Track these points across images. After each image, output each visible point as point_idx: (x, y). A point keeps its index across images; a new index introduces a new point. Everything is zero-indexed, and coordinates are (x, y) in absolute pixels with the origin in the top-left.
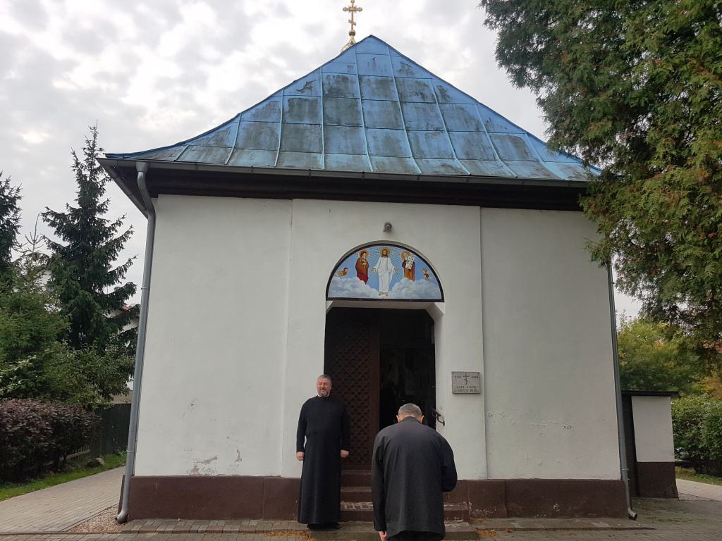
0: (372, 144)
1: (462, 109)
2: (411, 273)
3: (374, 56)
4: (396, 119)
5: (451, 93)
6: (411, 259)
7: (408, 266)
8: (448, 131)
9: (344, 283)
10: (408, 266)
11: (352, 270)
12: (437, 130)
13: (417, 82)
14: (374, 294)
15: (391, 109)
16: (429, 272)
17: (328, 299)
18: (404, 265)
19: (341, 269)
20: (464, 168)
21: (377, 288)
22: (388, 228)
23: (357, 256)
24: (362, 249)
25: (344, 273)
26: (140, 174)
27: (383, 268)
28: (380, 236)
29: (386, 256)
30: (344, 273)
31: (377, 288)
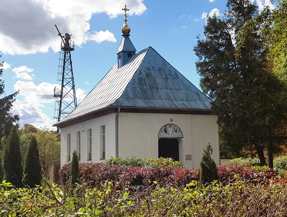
0: (164, 95)
1: (182, 81)
2: (176, 131)
3: (154, 57)
4: (167, 86)
5: (178, 74)
6: (176, 127)
7: (175, 129)
8: (180, 90)
9: (162, 134)
10: (175, 129)
11: (163, 131)
12: (178, 89)
13: (168, 70)
14: (168, 137)
15: (164, 81)
16: (180, 131)
17: (158, 138)
18: (174, 129)
19: (161, 130)
20: (188, 106)
21: (169, 135)
22: (171, 120)
23: (164, 127)
24: (165, 126)
25: (162, 132)
26: (119, 110)
27: (170, 130)
28: (170, 122)
29: (171, 127)
30: (162, 132)
31: (169, 135)
